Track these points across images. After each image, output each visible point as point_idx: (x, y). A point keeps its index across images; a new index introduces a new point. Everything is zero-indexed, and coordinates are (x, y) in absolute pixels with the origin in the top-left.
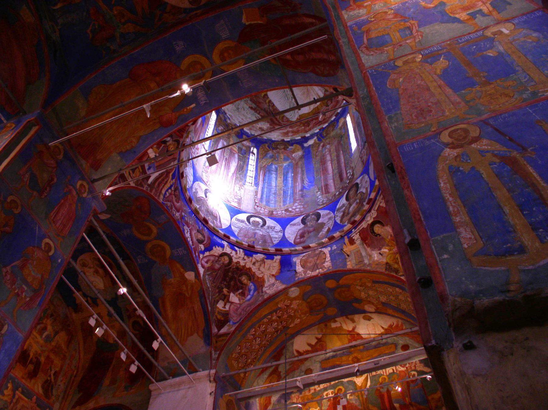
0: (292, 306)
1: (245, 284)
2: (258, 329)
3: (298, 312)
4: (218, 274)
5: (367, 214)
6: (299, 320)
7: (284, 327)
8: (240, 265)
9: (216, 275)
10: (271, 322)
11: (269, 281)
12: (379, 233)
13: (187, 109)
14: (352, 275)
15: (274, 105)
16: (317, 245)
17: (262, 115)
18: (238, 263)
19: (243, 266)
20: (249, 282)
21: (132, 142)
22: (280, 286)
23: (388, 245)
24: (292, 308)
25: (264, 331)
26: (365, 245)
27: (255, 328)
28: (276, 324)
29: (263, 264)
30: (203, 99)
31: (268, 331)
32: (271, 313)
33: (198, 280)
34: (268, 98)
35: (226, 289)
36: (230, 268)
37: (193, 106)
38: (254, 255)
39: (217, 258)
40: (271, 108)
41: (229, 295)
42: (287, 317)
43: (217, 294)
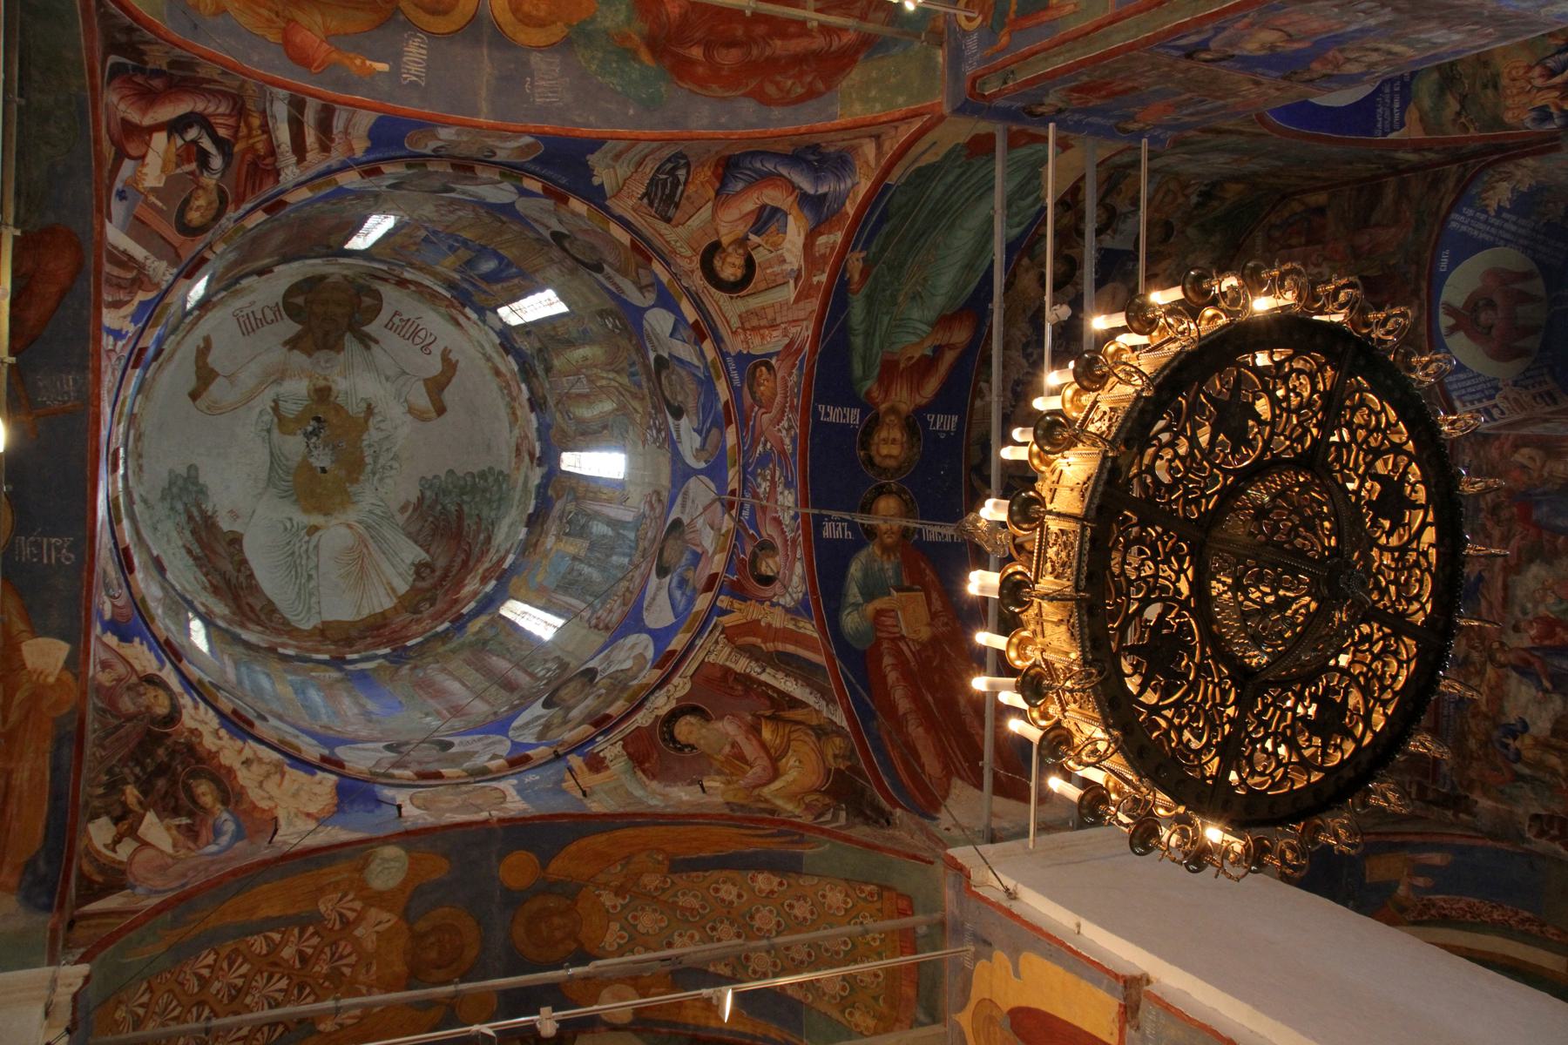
0: (359, 932)
1: (203, 808)
2: (225, 966)
3: (369, 965)
4: (122, 732)
5: (652, 693)
8: (200, 743)
9: (117, 728)
10: (272, 963)
11: (290, 823)
12: (692, 740)
14: (604, 837)
16: (465, 774)
17: (214, 581)
18: (194, 732)
19: (210, 752)
20: (219, 806)
23: (719, 772)
24: (357, 938)
25: (239, 990)
26: (640, 774)
27: (217, 954)
29: (278, 777)
30: (414, 68)
32: (282, 923)
33: (76, 677)
35: (136, 792)
36: (168, 735)
37: (382, 67)
38: (250, 742)
39: (134, 679)
40: (242, 579)
41: (142, 817)
42: (326, 977)
43: (101, 791)
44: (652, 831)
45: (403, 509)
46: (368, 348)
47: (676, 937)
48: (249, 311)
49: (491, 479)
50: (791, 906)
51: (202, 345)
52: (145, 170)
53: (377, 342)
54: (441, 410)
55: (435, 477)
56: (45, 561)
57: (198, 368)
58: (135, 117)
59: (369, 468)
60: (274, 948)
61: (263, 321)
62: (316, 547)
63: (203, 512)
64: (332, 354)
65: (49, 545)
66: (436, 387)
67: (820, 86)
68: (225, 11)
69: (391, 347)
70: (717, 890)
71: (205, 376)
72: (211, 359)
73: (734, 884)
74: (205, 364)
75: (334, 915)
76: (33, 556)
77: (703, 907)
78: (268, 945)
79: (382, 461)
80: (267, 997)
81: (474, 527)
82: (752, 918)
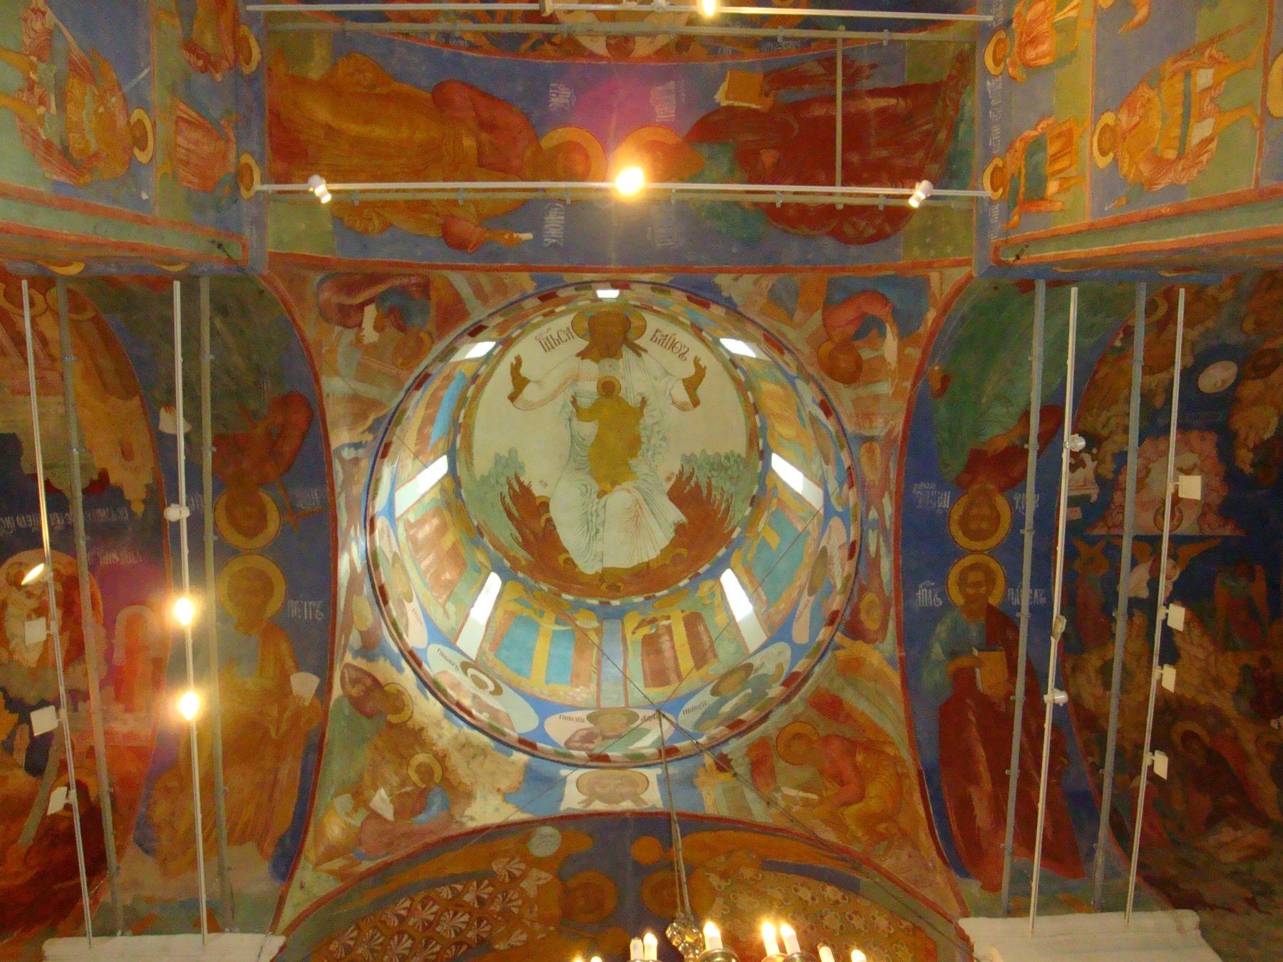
0: (523, 885)
2: (419, 907)
6: (524, 937)
7: (481, 941)
10: (457, 905)
13: (511, 236)
15: (555, 528)
21: (370, 220)
22: (512, 814)
25: (430, 923)
27: (413, 900)
28: (466, 918)
29: (482, 757)
30: (553, 232)
31: (438, 929)
32: (466, 878)
33: (322, 702)
34: (548, 511)
37: (527, 236)
42: (499, 914)
44: (746, 835)
45: (669, 479)
46: (639, 355)
48: (548, 335)
49: (731, 460)
50: (851, 918)
51: (515, 362)
52: (362, 334)
53: (645, 351)
54: (696, 403)
55: (692, 454)
56: (306, 617)
57: (514, 379)
58: (348, 301)
59: (644, 447)
60: (457, 895)
61: (559, 341)
62: (604, 506)
63: (521, 484)
64: (613, 360)
65: (308, 606)
66: (692, 385)
67: (888, 228)
68: (391, 225)
69: (656, 355)
70: (796, 890)
71: (519, 382)
72: (524, 371)
73: (809, 889)
74: (520, 375)
75: (504, 872)
76: (298, 614)
78: (453, 893)
79: (653, 441)
80: (453, 927)
81: (718, 497)
82: (822, 917)
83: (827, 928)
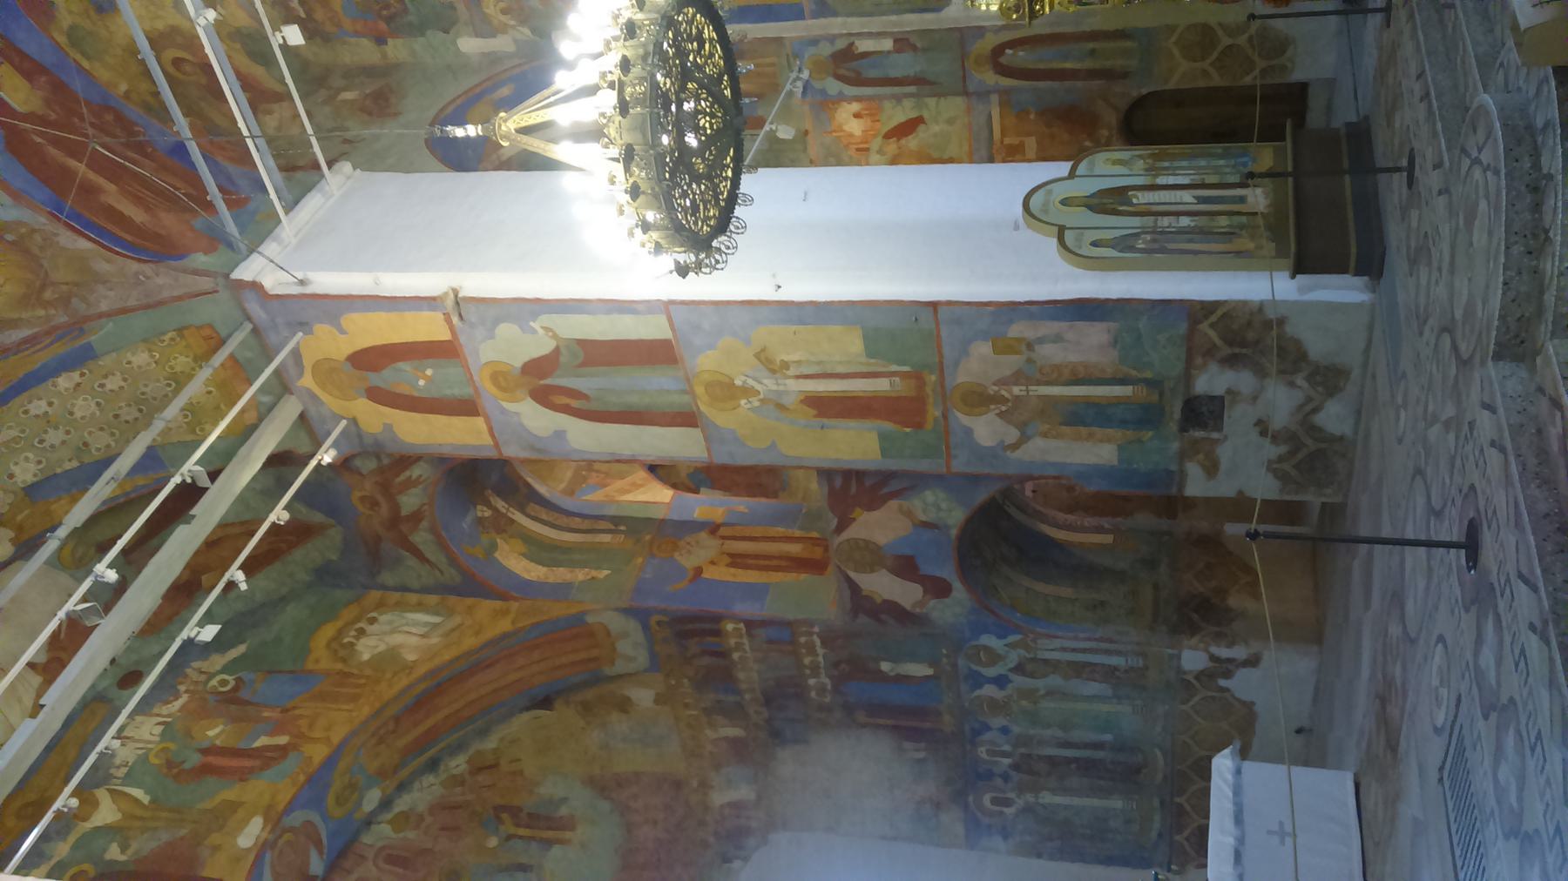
47: (13, 467)
50: (102, 386)
70: (26, 412)
77: (23, 431)
82: (71, 414)
83: (83, 418)
